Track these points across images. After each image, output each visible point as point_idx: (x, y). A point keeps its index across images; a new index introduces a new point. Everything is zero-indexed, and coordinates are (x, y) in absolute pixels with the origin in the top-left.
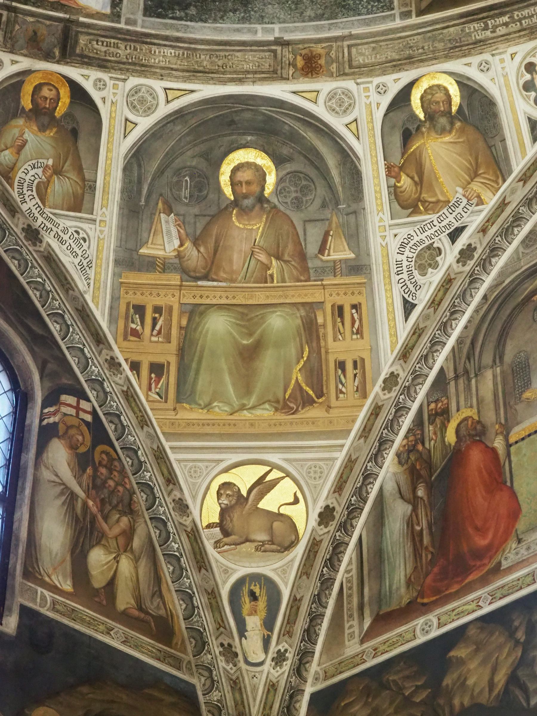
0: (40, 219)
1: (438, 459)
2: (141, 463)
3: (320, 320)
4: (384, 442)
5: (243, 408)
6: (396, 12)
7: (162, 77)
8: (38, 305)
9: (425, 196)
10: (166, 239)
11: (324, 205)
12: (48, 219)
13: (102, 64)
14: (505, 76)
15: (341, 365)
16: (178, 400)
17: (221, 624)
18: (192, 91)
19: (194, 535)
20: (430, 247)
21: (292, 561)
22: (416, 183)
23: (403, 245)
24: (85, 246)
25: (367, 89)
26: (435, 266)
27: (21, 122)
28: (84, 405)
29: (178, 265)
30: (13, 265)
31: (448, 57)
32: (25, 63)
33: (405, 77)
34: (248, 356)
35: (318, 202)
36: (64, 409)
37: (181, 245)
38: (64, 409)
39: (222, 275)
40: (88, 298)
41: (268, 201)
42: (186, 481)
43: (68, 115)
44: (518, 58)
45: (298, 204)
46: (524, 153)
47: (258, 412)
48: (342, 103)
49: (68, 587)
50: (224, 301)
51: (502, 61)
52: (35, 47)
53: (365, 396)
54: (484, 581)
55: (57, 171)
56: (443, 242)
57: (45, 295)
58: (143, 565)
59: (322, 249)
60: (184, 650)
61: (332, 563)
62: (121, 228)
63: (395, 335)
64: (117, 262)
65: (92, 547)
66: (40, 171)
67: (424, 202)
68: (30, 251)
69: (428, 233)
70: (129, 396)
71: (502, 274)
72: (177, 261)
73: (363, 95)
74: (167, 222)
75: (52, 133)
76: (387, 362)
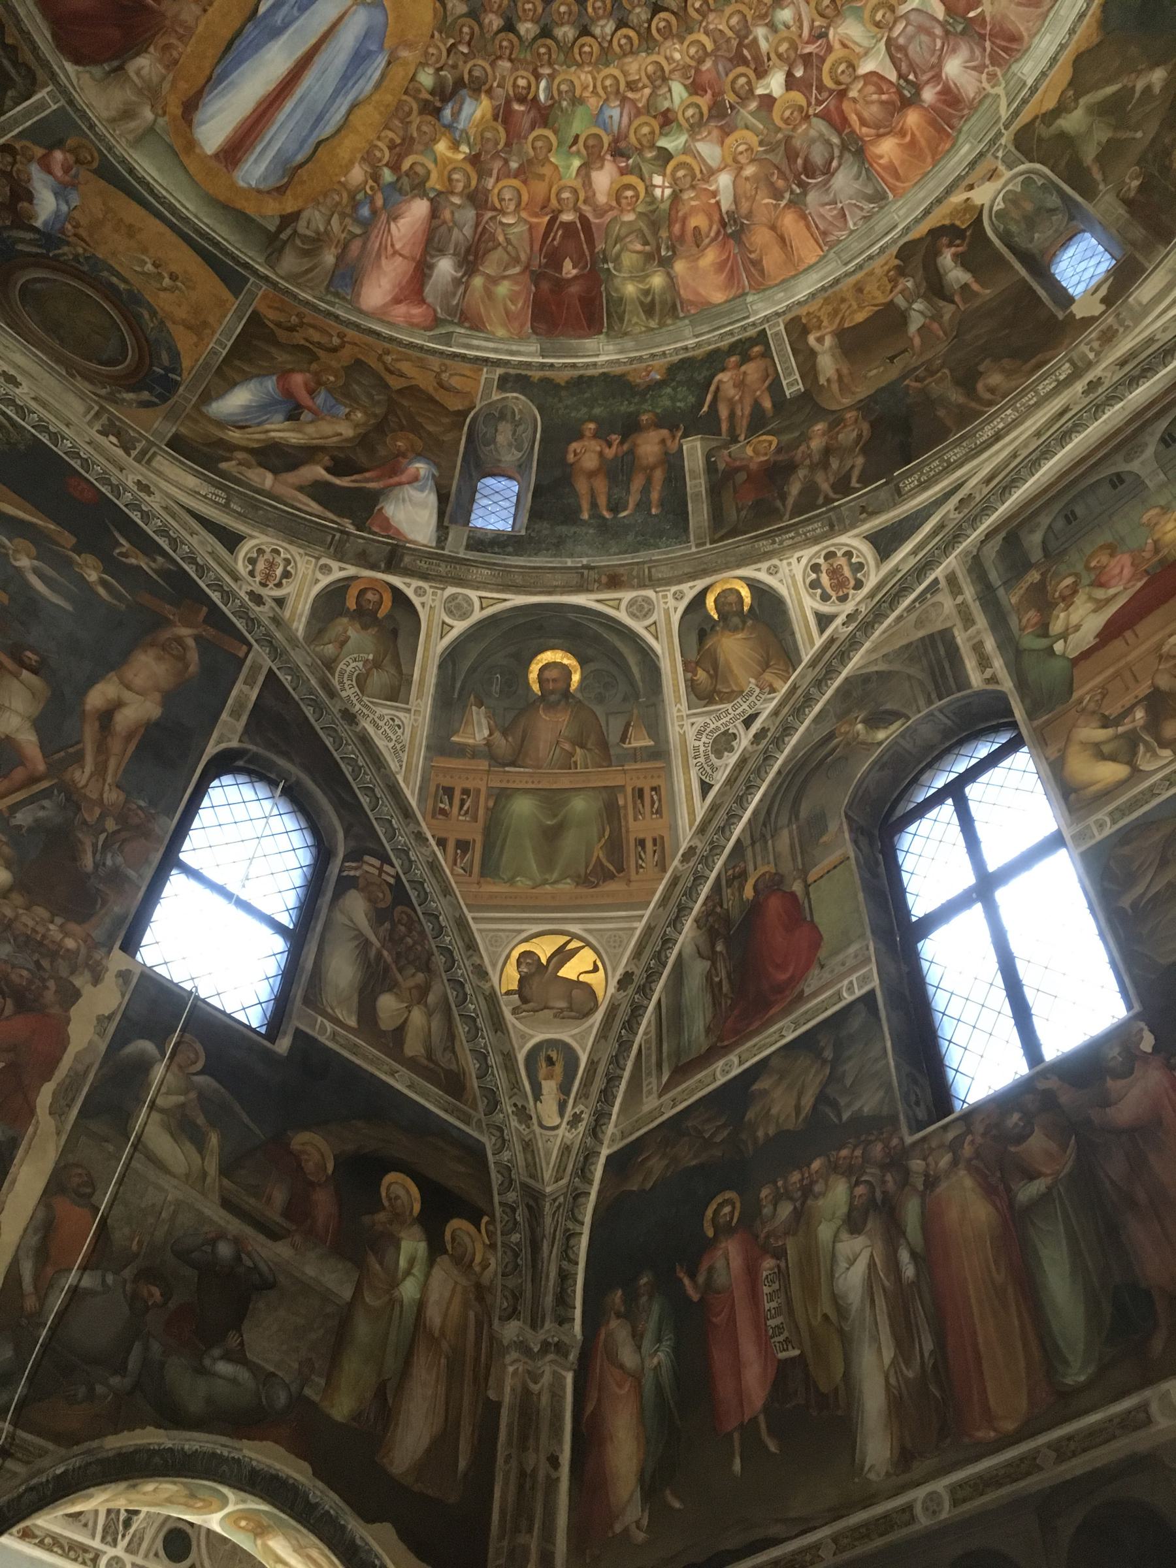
0: (358, 706)
1: (736, 915)
2: (441, 928)
3: (621, 802)
4: (682, 910)
6: (692, 544)
7: (477, 589)
8: (350, 778)
9: (719, 687)
10: (477, 730)
11: (625, 699)
12: (366, 706)
13: (424, 577)
14: (793, 577)
15: (642, 843)
16: (482, 874)
17: (515, 1085)
19: (492, 999)
20: (726, 733)
21: (591, 1026)
23: (700, 733)
24: (400, 732)
25: (665, 597)
26: (731, 750)
27: (345, 620)
28: (387, 868)
29: (488, 752)
30: (328, 742)
32: (351, 571)
33: (700, 584)
34: (551, 835)
36: (366, 867)
37: (491, 734)
38: (366, 867)
40: (400, 779)
41: (573, 696)
42: (487, 950)
43: (389, 616)
45: (601, 700)
46: (812, 644)
47: (560, 886)
48: (641, 609)
49: (352, 1022)
50: (530, 786)
51: (789, 564)
52: (362, 559)
53: (664, 870)
54: (786, 1012)
55: (377, 665)
57: (356, 771)
58: (436, 1023)
59: (624, 738)
60: (474, 1107)
61: (631, 1024)
62: (434, 718)
63: (692, 813)
64: (428, 748)
65: (383, 992)
66: (360, 664)
67: (719, 693)
68: (344, 730)
70: (434, 866)
71: (795, 749)
75: (373, 631)
76: (686, 836)
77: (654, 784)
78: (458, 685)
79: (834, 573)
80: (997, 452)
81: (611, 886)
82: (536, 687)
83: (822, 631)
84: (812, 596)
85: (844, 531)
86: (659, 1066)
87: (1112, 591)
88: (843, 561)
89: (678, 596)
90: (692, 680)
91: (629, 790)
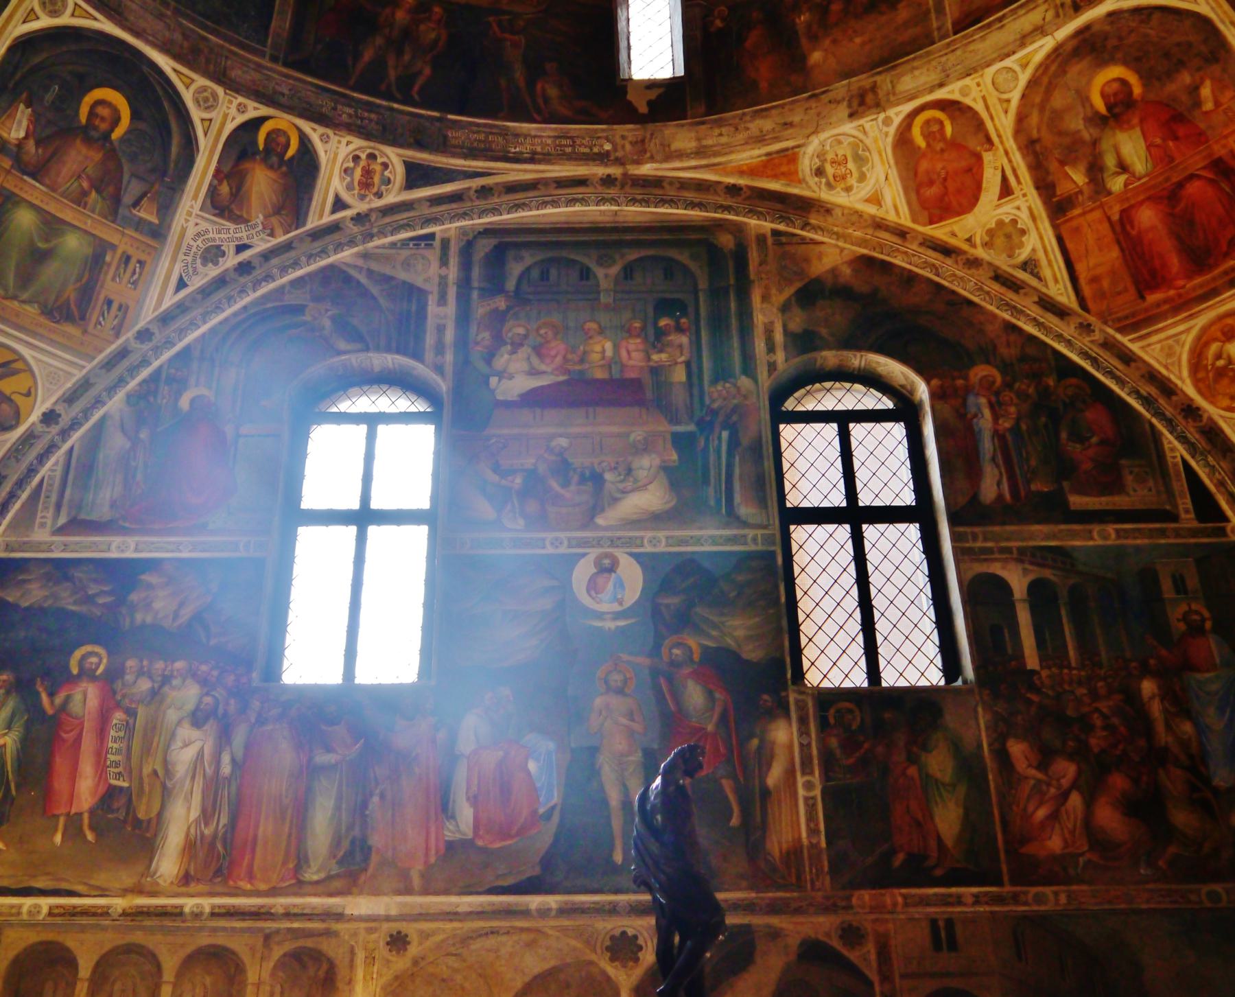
3: (108, 258)
5: (15, 298)
9: (233, 206)
11: (152, 171)
14: (336, 155)
15: (109, 303)
18: (95, 19)
20: (218, 247)
22: (231, 194)
23: (198, 235)
25: (231, 102)
26: (216, 264)
31: (301, 116)
35: (149, 165)
37: (26, 137)
39: (48, 182)
41: (111, 143)
44: (351, 147)
45: (133, 158)
46: (321, 216)
47: (27, 307)
48: (207, 102)
50: (37, 202)
51: (339, 142)
53: (117, 336)
56: (230, 249)
59: (136, 204)
67: (231, 211)
69: (222, 236)
72: (15, 149)
73: (226, 104)
74: (23, 112)
77: (143, 257)
78: (18, 76)
79: (367, 173)
80: (525, 171)
81: (70, 329)
82: (83, 118)
83: (333, 212)
84: (342, 179)
85: (394, 143)
86: (58, 507)
87: (543, 367)
88: (378, 168)
89: (241, 109)
90: (215, 188)
91: (119, 252)
